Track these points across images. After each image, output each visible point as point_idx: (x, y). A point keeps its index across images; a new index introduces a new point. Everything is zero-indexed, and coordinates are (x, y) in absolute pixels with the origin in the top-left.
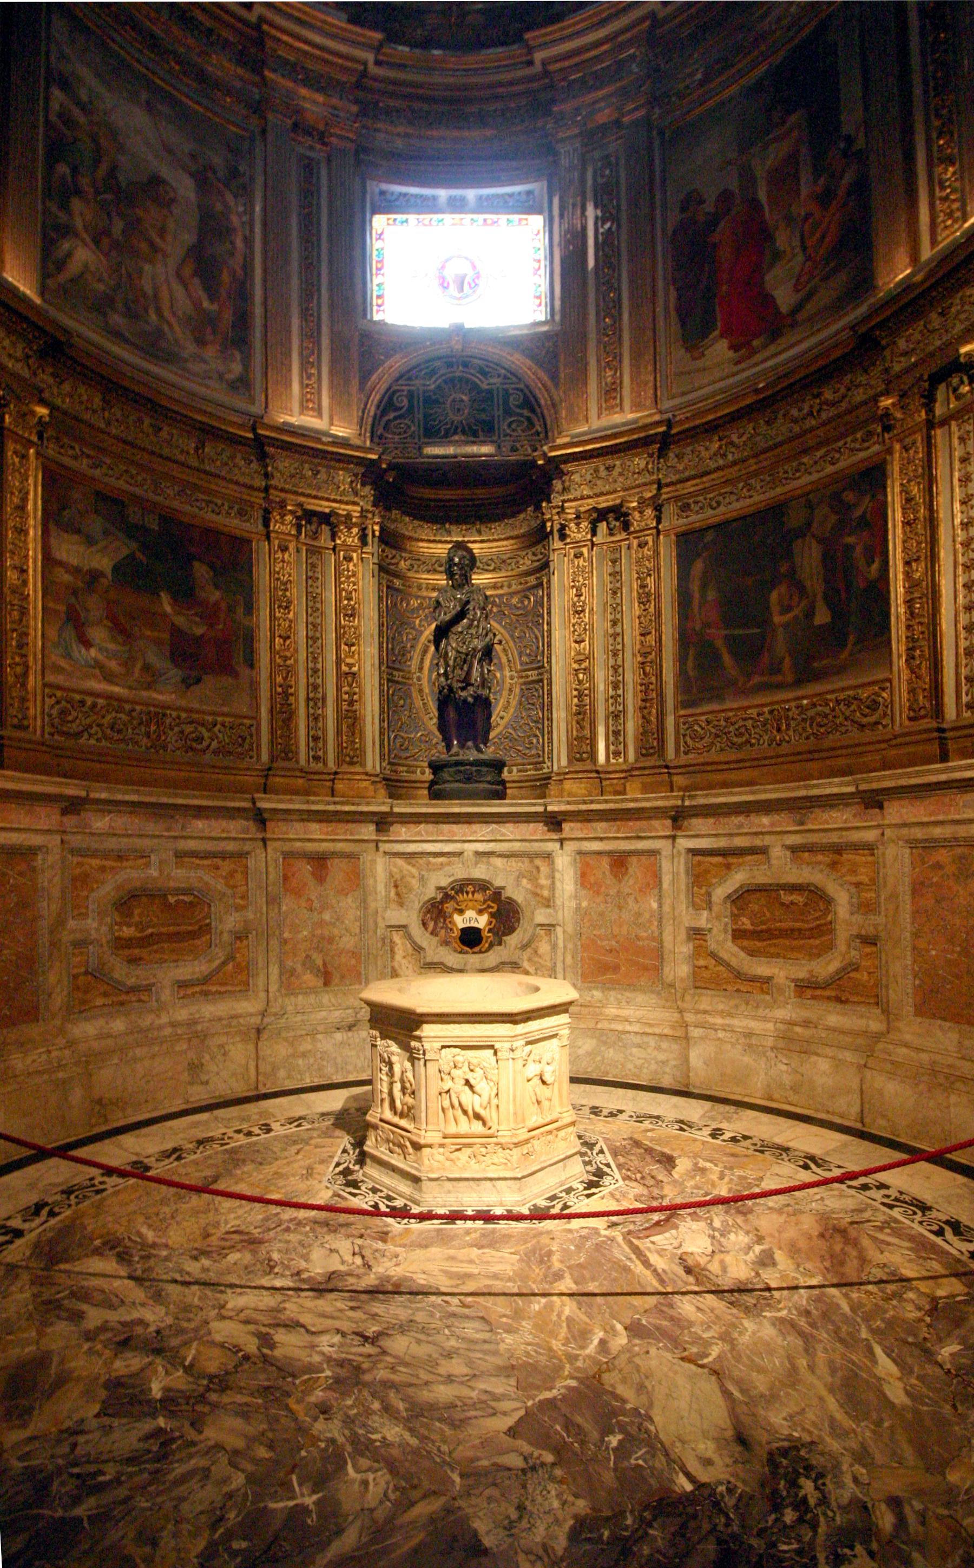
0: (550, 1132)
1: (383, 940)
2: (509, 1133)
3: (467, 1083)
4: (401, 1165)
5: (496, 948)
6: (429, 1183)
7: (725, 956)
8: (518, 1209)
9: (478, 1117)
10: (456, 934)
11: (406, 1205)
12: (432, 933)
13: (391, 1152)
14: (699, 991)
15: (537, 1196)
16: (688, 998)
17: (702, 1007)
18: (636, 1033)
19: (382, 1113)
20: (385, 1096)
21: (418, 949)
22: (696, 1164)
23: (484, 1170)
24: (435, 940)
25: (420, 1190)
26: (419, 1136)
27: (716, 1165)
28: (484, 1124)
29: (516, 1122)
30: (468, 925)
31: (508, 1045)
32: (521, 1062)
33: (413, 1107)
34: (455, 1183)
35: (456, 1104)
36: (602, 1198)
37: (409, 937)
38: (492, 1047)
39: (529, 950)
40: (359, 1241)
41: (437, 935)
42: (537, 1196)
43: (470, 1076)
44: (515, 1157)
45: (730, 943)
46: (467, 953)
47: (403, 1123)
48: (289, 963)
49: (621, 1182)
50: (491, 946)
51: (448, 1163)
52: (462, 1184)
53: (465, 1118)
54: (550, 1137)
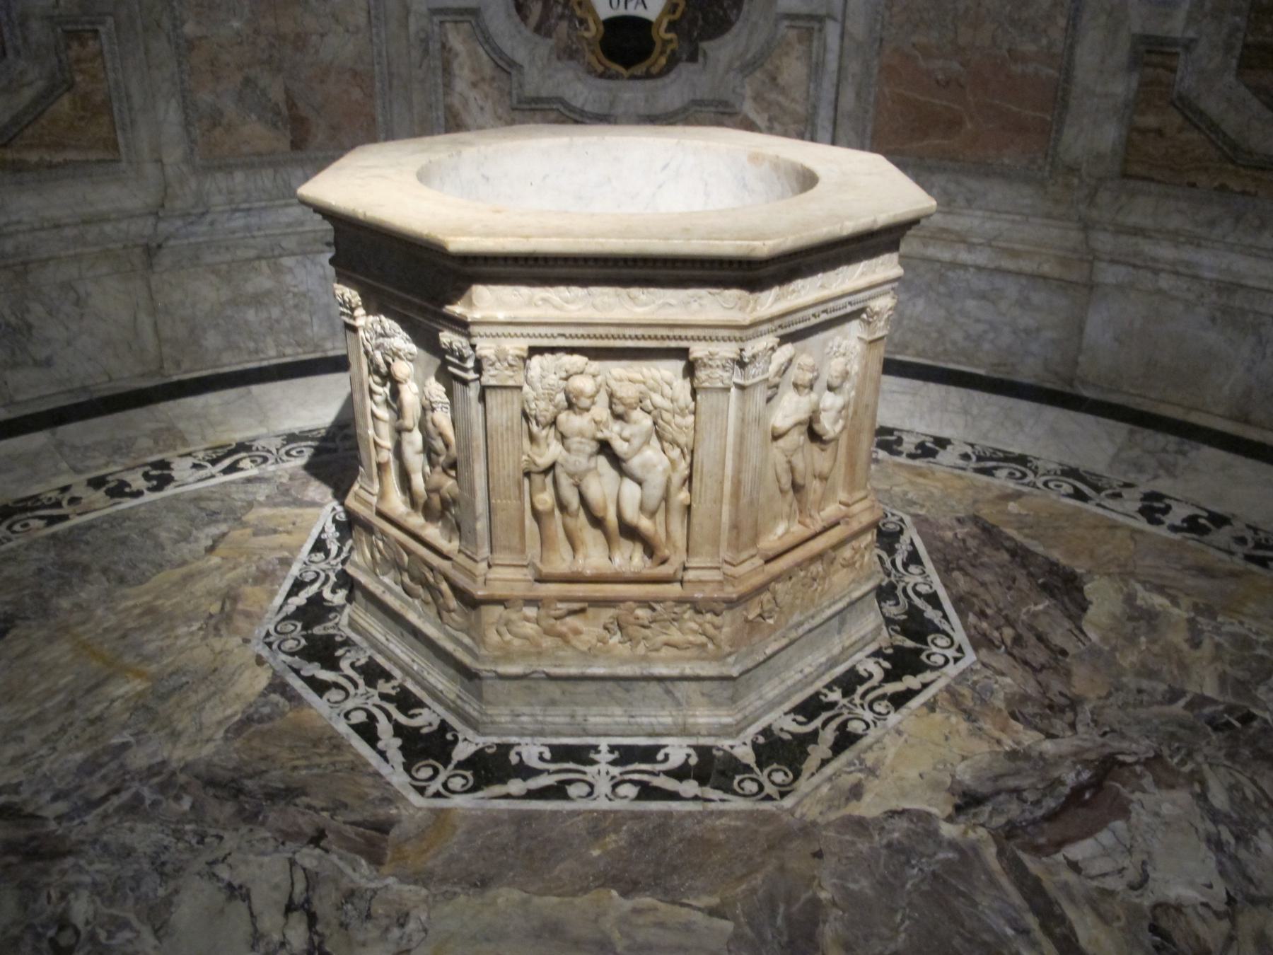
0: (819, 556)
1: (425, 42)
2: (714, 575)
3: (605, 447)
4: (430, 630)
5: (685, 69)
6: (500, 685)
7: (1212, 106)
8: (725, 743)
9: (630, 532)
10: (593, 32)
11: (444, 726)
12: (537, 29)
13: (408, 591)
14: (1131, 184)
15: (772, 705)
16: (1104, 197)
17: (1132, 220)
18: (979, 269)
19: (382, 496)
20: (387, 456)
21: (506, 66)
22: (1130, 599)
23: (644, 658)
24: (545, 47)
25: (479, 697)
26: (472, 575)
27: (1175, 602)
28: (650, 549)
29: (736, 546)
30: (621, 11)
31: (728, 351)
32: (759, 395)
33: (455, 502)
34: (568, 686)
35: (573, 501)
36: (931, 706)
37: (486, 39)
38: (682, 353)
39: (758, 74)
40: (309, 857)
41: (548, 35)
42: (772, 705)
43: (613, 433)
44: (726, 630)
45: (1230, 78)
46: (615, 77)
47: (433, 532)
48: (205, 97)
49: (970, 657)
50: (673, 61)
51: (548, 642)
52: (584, 687)
53: (598, 533)
54: (818, 568)
